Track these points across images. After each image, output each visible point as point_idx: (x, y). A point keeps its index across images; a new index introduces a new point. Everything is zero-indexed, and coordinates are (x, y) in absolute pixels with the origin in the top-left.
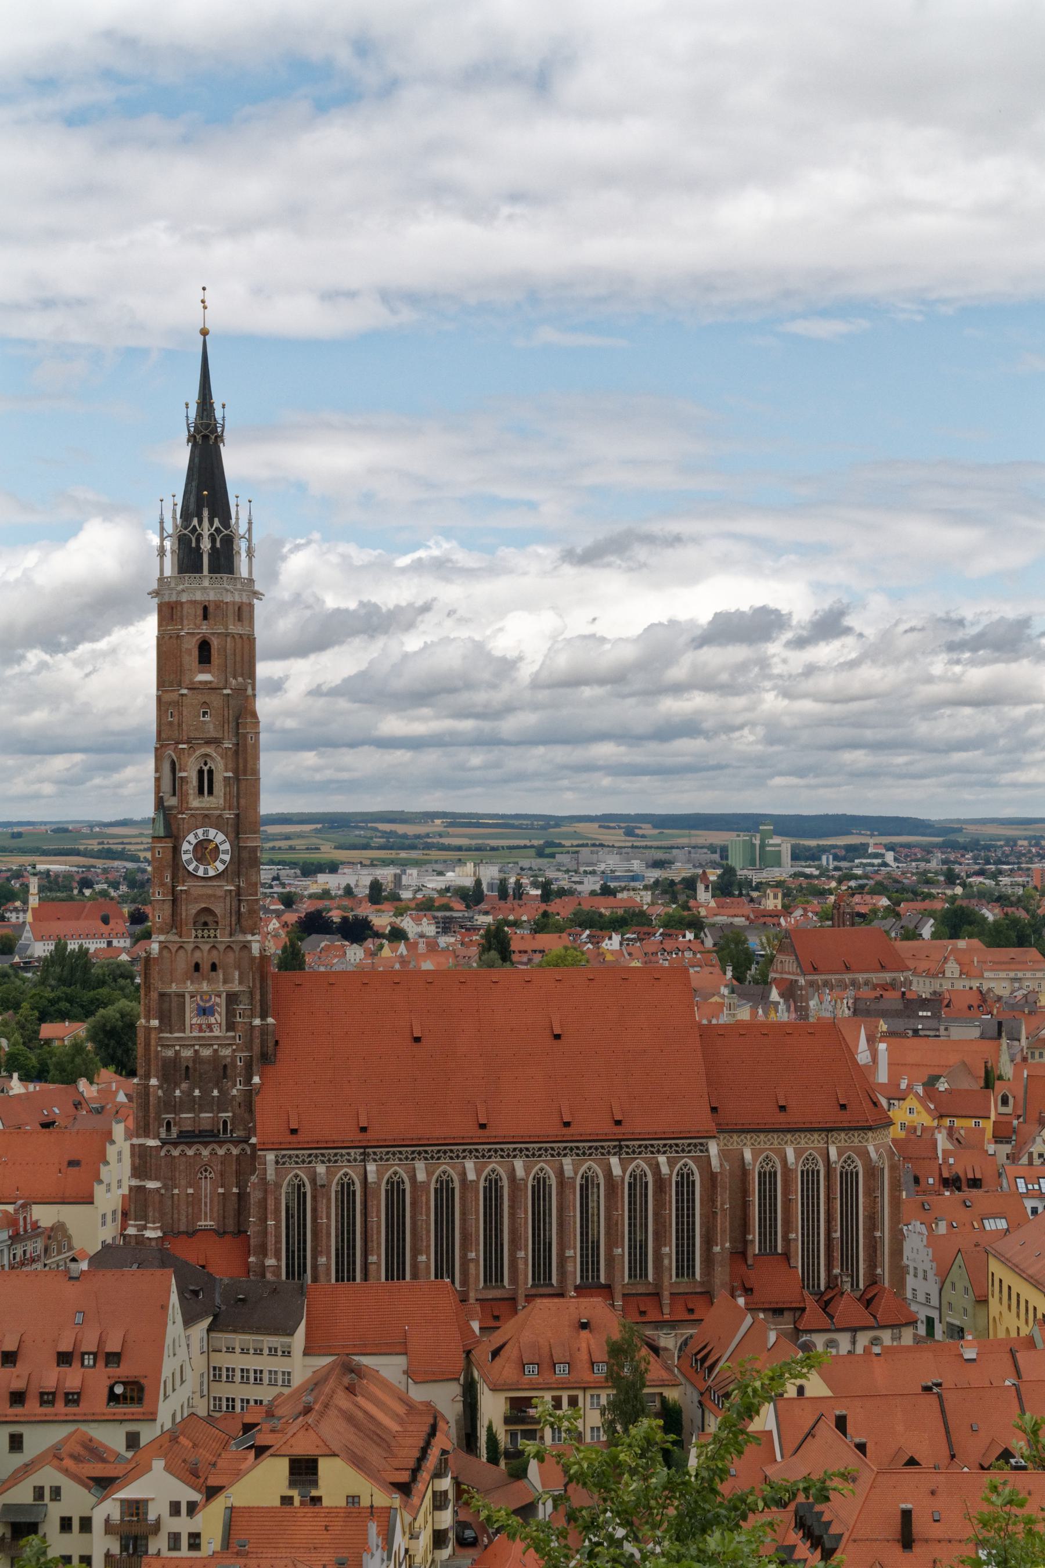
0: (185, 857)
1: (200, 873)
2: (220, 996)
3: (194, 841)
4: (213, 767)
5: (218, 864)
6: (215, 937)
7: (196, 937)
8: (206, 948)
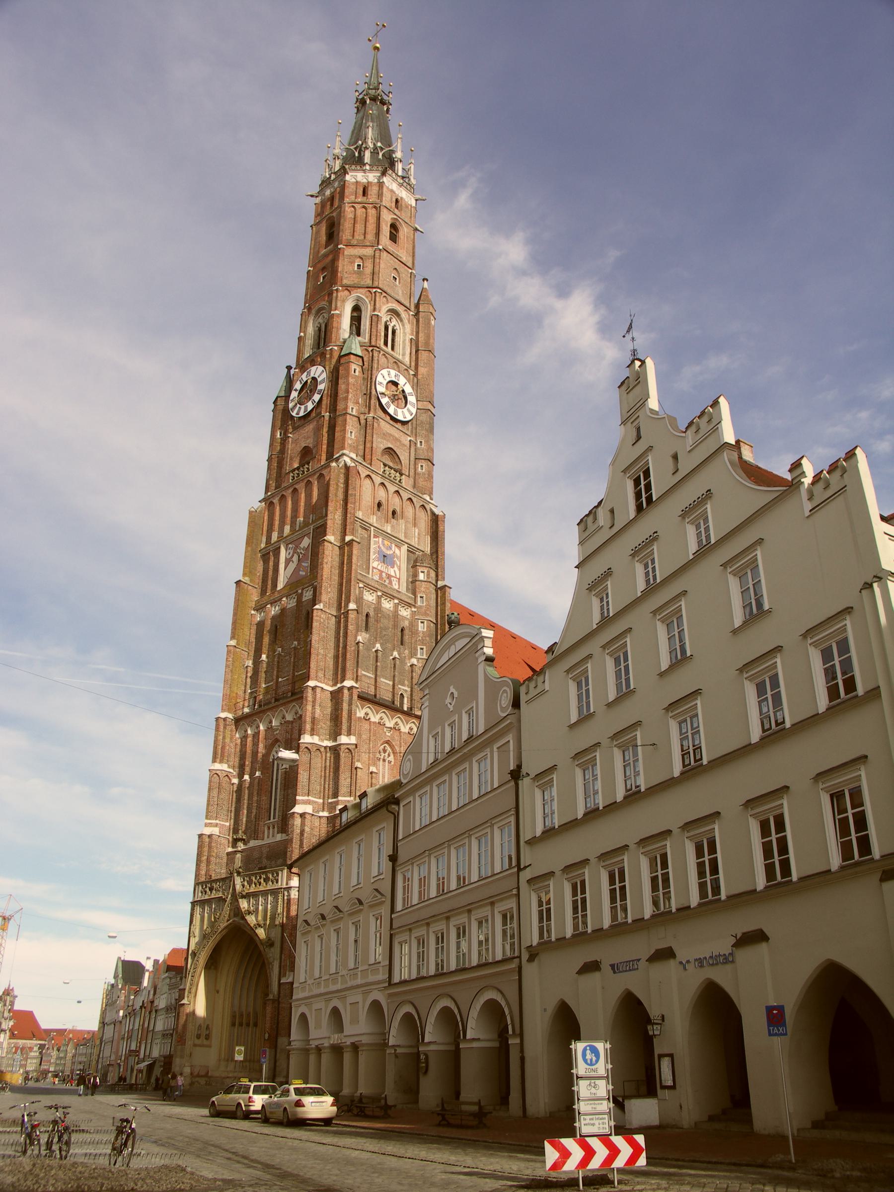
1: (391, 410)
2: (399, 548)
3: (388, 379)
4: (397, 327)
5: (405, 410)
8: (392, 488)
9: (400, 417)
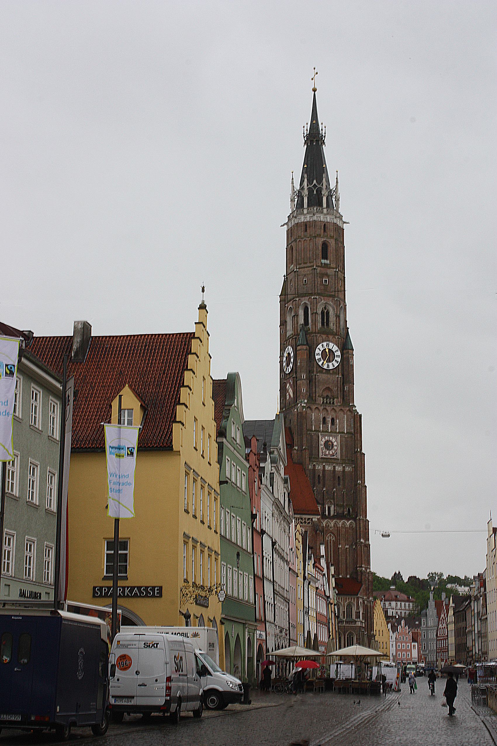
0: (317, 357)
1: (325, 367)
6: (333, 403)
7: (323, 402)
9: (331, 367)
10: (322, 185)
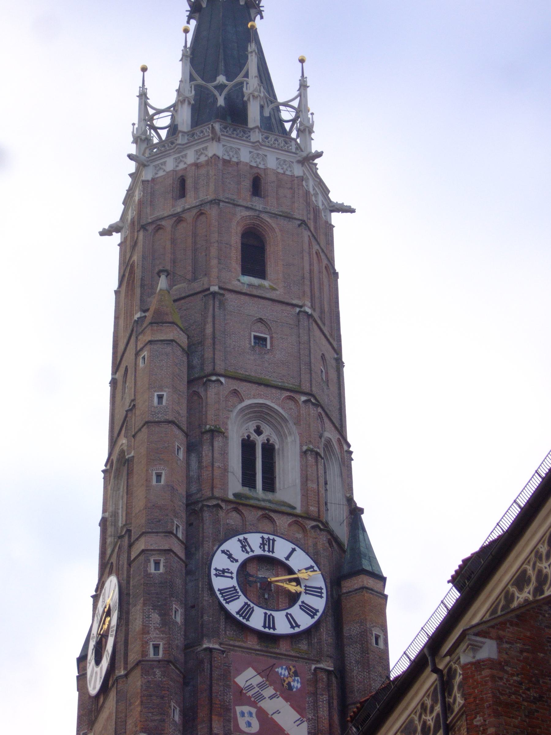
1: (256, 621)
3: (242, 557)
4: (275, 439)
5: (295, 611)
9: (282, 627)
10: (246, 75)
